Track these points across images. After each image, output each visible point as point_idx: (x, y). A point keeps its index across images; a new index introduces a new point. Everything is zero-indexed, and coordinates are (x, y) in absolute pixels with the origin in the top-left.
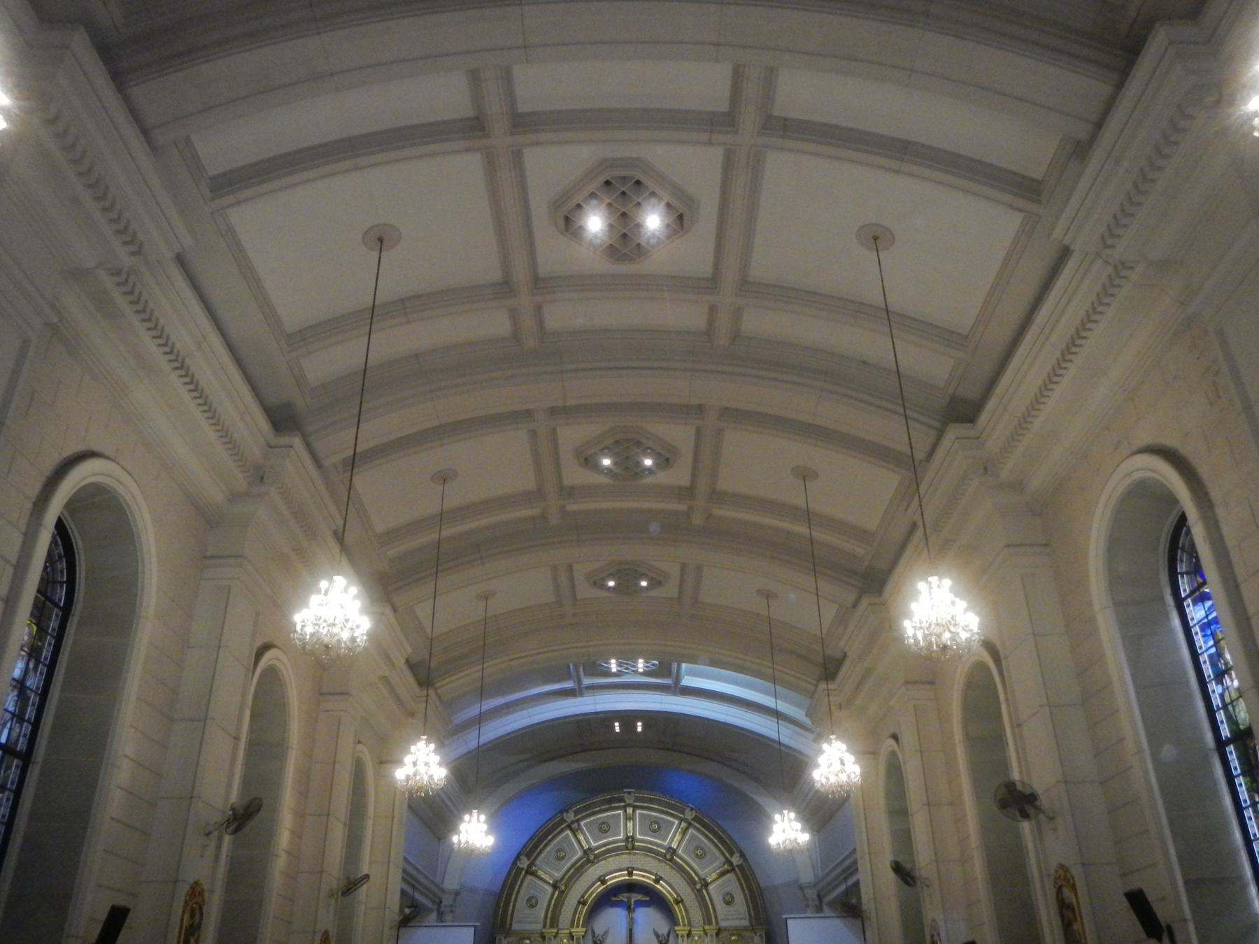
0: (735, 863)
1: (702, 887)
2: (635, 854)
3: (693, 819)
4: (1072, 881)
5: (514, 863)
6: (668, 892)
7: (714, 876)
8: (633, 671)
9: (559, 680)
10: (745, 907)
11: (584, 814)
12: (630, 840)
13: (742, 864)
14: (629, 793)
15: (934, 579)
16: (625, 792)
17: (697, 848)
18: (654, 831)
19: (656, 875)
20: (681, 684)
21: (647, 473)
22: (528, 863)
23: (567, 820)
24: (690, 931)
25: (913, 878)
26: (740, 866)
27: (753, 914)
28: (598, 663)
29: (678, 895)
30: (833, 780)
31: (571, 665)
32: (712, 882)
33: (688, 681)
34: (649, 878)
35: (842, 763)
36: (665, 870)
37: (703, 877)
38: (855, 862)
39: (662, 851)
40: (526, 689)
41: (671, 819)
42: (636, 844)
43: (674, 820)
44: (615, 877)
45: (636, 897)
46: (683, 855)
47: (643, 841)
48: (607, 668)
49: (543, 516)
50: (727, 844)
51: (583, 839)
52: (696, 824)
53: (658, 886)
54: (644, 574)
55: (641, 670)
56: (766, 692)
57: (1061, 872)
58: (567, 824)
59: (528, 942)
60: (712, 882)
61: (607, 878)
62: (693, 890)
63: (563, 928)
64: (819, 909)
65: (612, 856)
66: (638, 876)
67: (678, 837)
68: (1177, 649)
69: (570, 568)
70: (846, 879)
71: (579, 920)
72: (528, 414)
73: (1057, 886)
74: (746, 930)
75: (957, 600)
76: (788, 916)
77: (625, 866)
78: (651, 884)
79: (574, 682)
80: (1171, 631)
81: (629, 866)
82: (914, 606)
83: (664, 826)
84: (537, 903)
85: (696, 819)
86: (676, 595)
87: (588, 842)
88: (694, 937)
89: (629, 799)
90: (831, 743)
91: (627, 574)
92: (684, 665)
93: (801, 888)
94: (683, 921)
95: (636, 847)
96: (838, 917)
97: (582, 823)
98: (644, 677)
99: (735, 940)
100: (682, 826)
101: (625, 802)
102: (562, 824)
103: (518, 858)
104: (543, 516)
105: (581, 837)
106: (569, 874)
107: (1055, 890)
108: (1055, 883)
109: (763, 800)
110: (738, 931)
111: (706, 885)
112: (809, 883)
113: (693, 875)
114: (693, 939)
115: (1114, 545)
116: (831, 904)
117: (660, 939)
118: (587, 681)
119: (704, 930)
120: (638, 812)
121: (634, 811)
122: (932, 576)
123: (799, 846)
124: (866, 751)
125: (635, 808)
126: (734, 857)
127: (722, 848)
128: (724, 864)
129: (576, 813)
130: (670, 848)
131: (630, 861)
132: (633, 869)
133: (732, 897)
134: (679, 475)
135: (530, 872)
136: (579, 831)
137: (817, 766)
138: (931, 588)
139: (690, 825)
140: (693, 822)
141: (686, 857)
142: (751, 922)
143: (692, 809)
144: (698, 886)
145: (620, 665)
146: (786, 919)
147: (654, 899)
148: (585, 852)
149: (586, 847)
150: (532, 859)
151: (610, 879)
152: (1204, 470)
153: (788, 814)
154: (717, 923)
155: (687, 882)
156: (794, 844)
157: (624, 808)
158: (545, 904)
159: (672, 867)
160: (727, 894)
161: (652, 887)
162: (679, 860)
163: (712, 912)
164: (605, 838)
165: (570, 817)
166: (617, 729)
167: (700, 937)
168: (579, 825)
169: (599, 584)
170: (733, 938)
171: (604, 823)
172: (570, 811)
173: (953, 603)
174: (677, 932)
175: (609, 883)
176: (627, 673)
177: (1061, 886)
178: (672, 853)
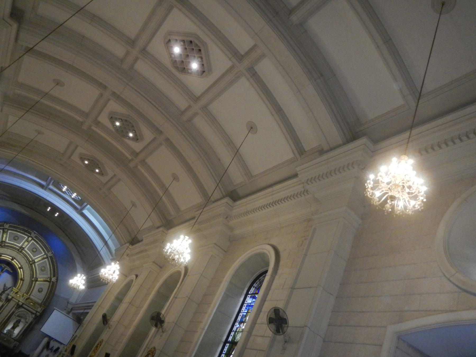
0: (52, 280)
1: (35, 280)
2: (20, 254)
3: (50, 257)
4: (154, 354)
6: (21, 274)
7: (42, 279)
8: (70, 195)
9: (43, 180)
10: (44, 297)
11: (12, 229)
12: (22, 248)
13: (55, 282)
14: (35, 233)
15: (187, 237)
16: (33, 232)
18: (33, 251)
19: (21, 266)
20: (83, 211)
21: (128, 137)
23: (5, 225)
24: (18, 292)
25: (107, 322)
26: (53, 283)
27: (45, 300)
28: (60, 183)
29: (24, 277)
30: (107, 275)
31: (50, 177)
33: (85, 212)
35: (114, 272)
36: (26, 267)
37: (37, 277)
38: (93, 306)
39: (30, 259)
40: (27, 173)
41: (42, 252)
42: (23, 251)
43: (43, 253)
45: (8, 268)
46: (37, 265)
47: (26, 252)
48: (62, 187)
49: (82, 123)
50: (55, 272)
51: (5, 236)
52: (49, 259)
54: (100, 168)
55: (73, 197)
56: (108, 234)
57: (153, 349)
62: (30, 279)
64: (68, 313)
65: (10, 249)
66: (15, 262)
67: (39, 259)
68: (236, 307)
69: (77, 147)
70: (85, 309)
72: (105, 87)
73: (149, 353)
75: (189, 248)
76: (55, 308)
77: (13, 256)
78: (17, 268)
79: (46, 184)
80: (239, 300)
81: (14, 256)
82: (175, 241)
85: (50, 257)
86: (104, 183)
87: (6, 239)
89: (33, 235)
90: (116, 264)
91: (94, 163)
92: (88, 206)
93: (68, 303)
94: (18, 287)
95: (22, 252)
96: (73, 319)
97: (9, 231)
98: (72, 200)
99: (31, 305)
100: (44, 256)
101: (31, 235)
104: (82, 123)
105: (5, 236)
107: (147, 354)
108: (149, 352)
109: (78, 266)
110: (35, 303)
111: (36, 280)
112: (72, 303)
113: (35, 274)
114: (16, 295)
115: (243, 265)
116: (74, 314)
117: (5, 288)
118: (51, 187)
119: (23, 295)
120: (33, 241)
121: (31, 240)
122: (188, 236)
123: (79, 289)
124: (124, 274)
125: (33, 239)
126: (54, 278)
128: (48, 278)
129: (10, 226)
130: (34, 261)
131: (16, 255)
132: (15, 259)
134: (137, 147)
136: (6, 233)
137: (105, 268)
138: (184, 239)
139: (47, 258)
140: (49, 257)
141: (37, 267)
142: (42, 302)
143: (52, 253)
144: (33, 279)
145: (67, 190)
146: (55, 309)
147: (14, 273)
149: (4, 240)
152: (282, 263)
153: (84, 276)
155: (30, 275)
156: (77, 287)
157: (29, 237)
159: (29, 267)
163: (31, 290)
164: (14, 242)
165: (7, 226)
166: (48, 210)
167: (20, 296)
168: (7, 231)
169: (82, 160)
170: (31, 304)
171: (16, 236)
172: (8, 224)
173: (187, 248)
174: (13, 289)
175: (2, 257)
176: (67, 194)
177: (150, 354)
178: (33, 263)
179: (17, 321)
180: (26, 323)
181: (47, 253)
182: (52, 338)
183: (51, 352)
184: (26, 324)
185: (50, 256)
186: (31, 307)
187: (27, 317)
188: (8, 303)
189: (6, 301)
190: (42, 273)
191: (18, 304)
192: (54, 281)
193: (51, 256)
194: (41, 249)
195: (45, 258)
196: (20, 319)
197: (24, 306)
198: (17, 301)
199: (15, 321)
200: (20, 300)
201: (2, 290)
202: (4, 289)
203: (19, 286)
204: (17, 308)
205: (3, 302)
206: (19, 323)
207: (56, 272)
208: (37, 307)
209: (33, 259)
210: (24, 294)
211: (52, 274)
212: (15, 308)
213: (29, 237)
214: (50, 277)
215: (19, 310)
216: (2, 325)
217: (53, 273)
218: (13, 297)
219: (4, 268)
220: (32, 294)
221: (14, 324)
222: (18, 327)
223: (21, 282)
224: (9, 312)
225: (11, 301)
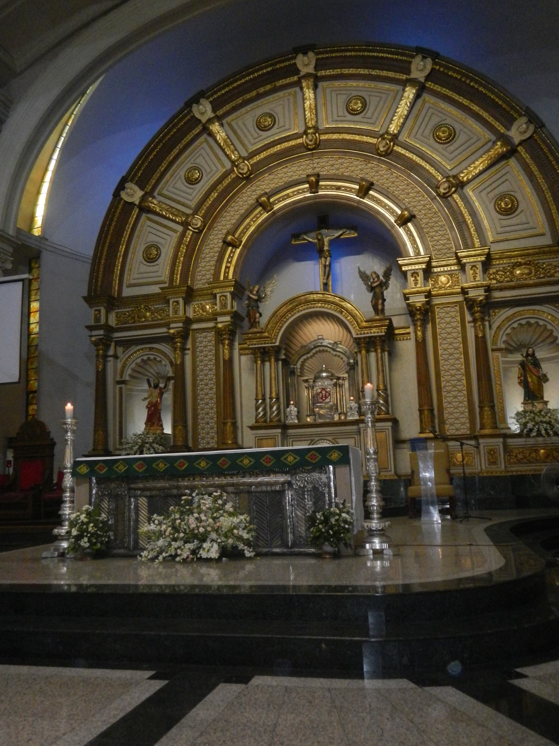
0: (516, 141)
1: (450, 188)
3: (428, 78)
5: (116, 195)
6: (384, 206)
17: (438, 127)
22: (140, 193)
24: (429, 263)
32: (469, 181)
34: (350, 190)
37: (451, 173)
41: (387, 86)
42: (323, 137)
44: (288, 196)
53: (365, 201)
58: (200, 127)
59: (148, 314)
60: (469, 181)
61: (271, 200)
62: (433, 199)
63: (199, 286)
65: (279, 165)
71: (227, 273)
74: (545, 253)
83: (372, 102)
84: (159, 255)
85: (431, 77)
88: (439, 274)
94: (418, 254)
97: (229, 119)
99: (522, 274)
100: (406, 94)
102: (197, 126)
103: (121, 187)
106: (209, 202)
111: (461, 185)
114: (436, 282)
127: (490, 119)
128: (494, 143)
130: (387, 133)
135: (144, 209)
139: (421, 90)
140: (428, 84)
143: (424, 58)
148: (233, 162)
150: (149, 188)
151: (279, 201)
154: (483, 243)
155: (422, 187)
157: (298, 84)
158: (171, 254)
160: (501, 197)
161: (356, 204)
162: (403, 152)
172: (202, 101)
174: (404, 269)
179: (523, 365)
181: (404, 77)
185: (427, 71)
186: (531, 282)
187: (549, 327)
188: (429, 326)
189: (419, 323)
190: (452, 148)
191: (471, 304)
192: (527, 135)
193: (433, 69)
194: (372, 84)
195: (418, 96)
196: (528, 355)
197: (497, 295)
198: (460, 298)
199: (515, 372)
200: (465, 285)
201: (370, 295)
202: (372, 289)
203: (416, 249)
204: (483, 320)
205: (412, 336)
206: (536, 364)
207: (504, 101)
208: (555, 266)
209: (381, 133)
210: (456, 254)
211: (497, 125)
212: (475, 327)
213: (298, 84)
214: (493, 138)
215: (495, 326)
216: (481, 408)
217: (493, 117)
218: (429, 295)
219: (321, 241)
220: (490, 237)
221: (524, 383)
222: (546, 386)
223: (409, 230)
225: (433, 312)
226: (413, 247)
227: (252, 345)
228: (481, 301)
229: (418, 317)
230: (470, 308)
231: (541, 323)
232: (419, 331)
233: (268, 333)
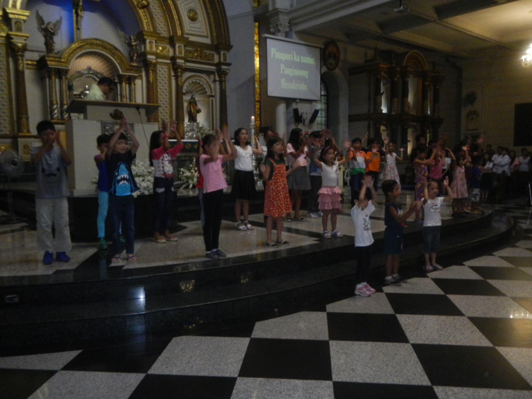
27: (215, 34)
64: (287, 35)
112: (286, 10)
133: (196, 13)
180: (211, 98)
182: (294, 100)
183: (304, 124)
184: (212, 100)
186: (202, 61)
196: (192, 98)
198: (168, 61)
224: (170, 93)
226: (147, 25)
227: (51, 65)
228: (182, 66)
229: (152, 68)
230: (175, 70)
231: (201, 83)
232: (151, 76)
233: (64, 59)
